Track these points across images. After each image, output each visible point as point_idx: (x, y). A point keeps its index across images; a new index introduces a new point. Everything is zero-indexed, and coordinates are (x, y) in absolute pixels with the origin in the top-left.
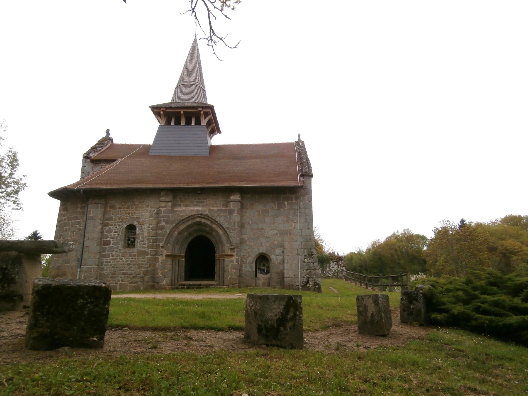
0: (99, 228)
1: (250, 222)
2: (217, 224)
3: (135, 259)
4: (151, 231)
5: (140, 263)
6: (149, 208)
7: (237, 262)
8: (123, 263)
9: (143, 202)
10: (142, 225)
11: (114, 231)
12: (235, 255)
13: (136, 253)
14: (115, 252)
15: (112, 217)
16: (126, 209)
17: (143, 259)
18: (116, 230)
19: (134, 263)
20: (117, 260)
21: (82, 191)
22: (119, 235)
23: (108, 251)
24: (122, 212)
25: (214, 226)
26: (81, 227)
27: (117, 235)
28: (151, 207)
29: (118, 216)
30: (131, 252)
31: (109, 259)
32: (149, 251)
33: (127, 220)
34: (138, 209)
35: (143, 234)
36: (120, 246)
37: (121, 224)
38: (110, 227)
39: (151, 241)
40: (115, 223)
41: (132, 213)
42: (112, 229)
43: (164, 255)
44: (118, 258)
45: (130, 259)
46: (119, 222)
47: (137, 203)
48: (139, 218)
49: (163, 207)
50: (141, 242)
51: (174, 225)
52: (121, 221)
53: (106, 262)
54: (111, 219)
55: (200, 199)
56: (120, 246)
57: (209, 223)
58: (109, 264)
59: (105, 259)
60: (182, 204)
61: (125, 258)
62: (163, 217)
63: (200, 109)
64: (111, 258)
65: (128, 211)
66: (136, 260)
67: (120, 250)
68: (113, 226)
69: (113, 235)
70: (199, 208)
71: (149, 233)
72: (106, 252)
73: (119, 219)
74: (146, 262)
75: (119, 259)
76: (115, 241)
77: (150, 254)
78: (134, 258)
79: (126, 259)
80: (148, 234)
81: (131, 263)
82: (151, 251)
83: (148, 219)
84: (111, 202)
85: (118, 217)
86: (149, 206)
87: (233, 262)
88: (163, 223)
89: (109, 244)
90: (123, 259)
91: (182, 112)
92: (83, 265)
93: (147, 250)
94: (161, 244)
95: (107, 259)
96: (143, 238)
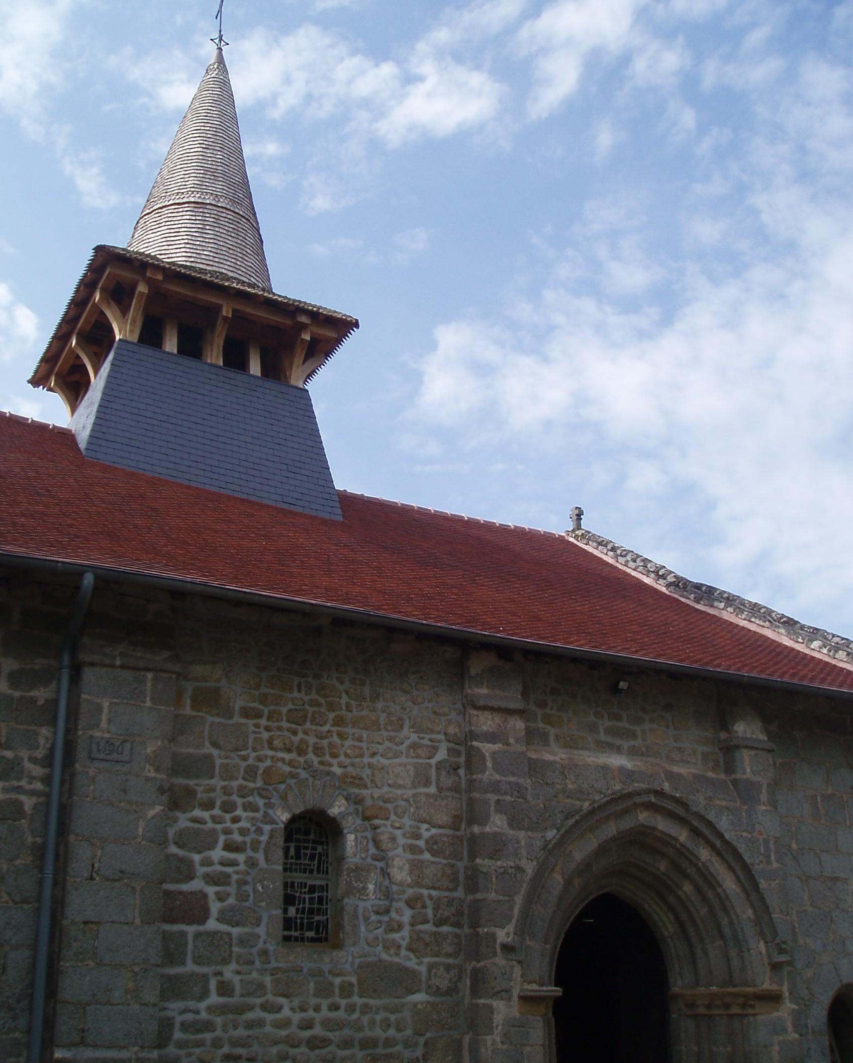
0: (151, 813)
1: (794, 846)
2: (718, 843)
3: (351, 1009)
4: (427, 856)
5: (378, 1032)
6: (409, 736)
7: (797, 1027)
8: (283, 1033)
9: (375, 698)
10: (376, 822)
11: (222, 838)
12: (787, 994)
13: (354, 980)
14: (234, 966)
15: (209, 757)
16: (285, 724)
17: (395, 1010)
18: (237, 838)
19: (346, 1031)
20: (250, 1016)
21: (89, 579)
22: (252, 863)
23: (197, 961)
24: (265, 735)
25: (704, 854)
26: (23, 798)
27: (242, 867)
28: (419, 730)
29: (245, 758)
30: (326, 968)
31: (203, 1005)
32: (419, 965)
33: (292, 782)
34: (349, 730)
35: (385, 873)
36: (261, 930)
37: (261, 802)
38: (197, 813)
39: (429, 912)
40: (226, 791)
41: (318, 750)
42: (210, 825)
43: (516, 993)
44: (258, 1001)
45: (324, 1008)
46: (251, 792)
47: (345, 699)
48: (358, 782)
49: (491, 738)
50: (374, 917)
51: (551, 834)
52: (259, 783)
53: (185, 1027)
54: (204, 767)
55: (618, 718)
56: (261, 930)
57: (683, 836)
58: (208, 1036)
59: (181, 1005)
60: (552, 731)
61: (296, 1002)
62: (495, 787)
63: (304, 319)
64: (214, 999)
65: (295, 733)
66: (356, 1015)
67: (264, 953)
68: (217, 812)
69: (222, 863)
70: (617, 761)
71: (416, 867)
72: (184, 963)
73: (251, 773)
74: (409, 1032)
75: (264, 1008)
76: (231, 901)
77: (429, 987)
78: (343, 1002)
79: (303, 1009)
80: (411, 872)
81: (330, 1035)
82: (431, 967)
83: (410, 792)
84: (198, 670)
85: (243, 764)
86: (407, 724)
87: (784, 1030)
88: (497, 823)
89: (203, 918)
90: (286, 1012)
91: (226, 312)
92: (68, 1046)
93: (409, 964)
94: (503, 935)
95: (192, 1004)
96: (387, 895)
